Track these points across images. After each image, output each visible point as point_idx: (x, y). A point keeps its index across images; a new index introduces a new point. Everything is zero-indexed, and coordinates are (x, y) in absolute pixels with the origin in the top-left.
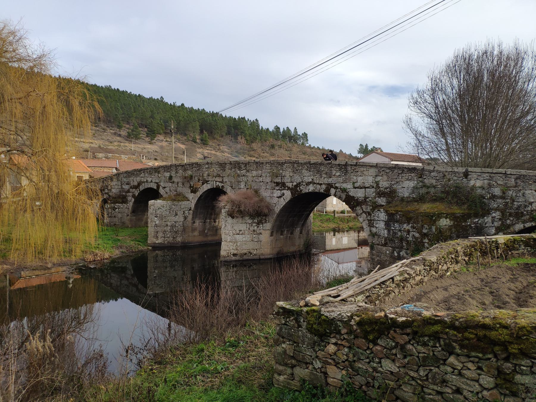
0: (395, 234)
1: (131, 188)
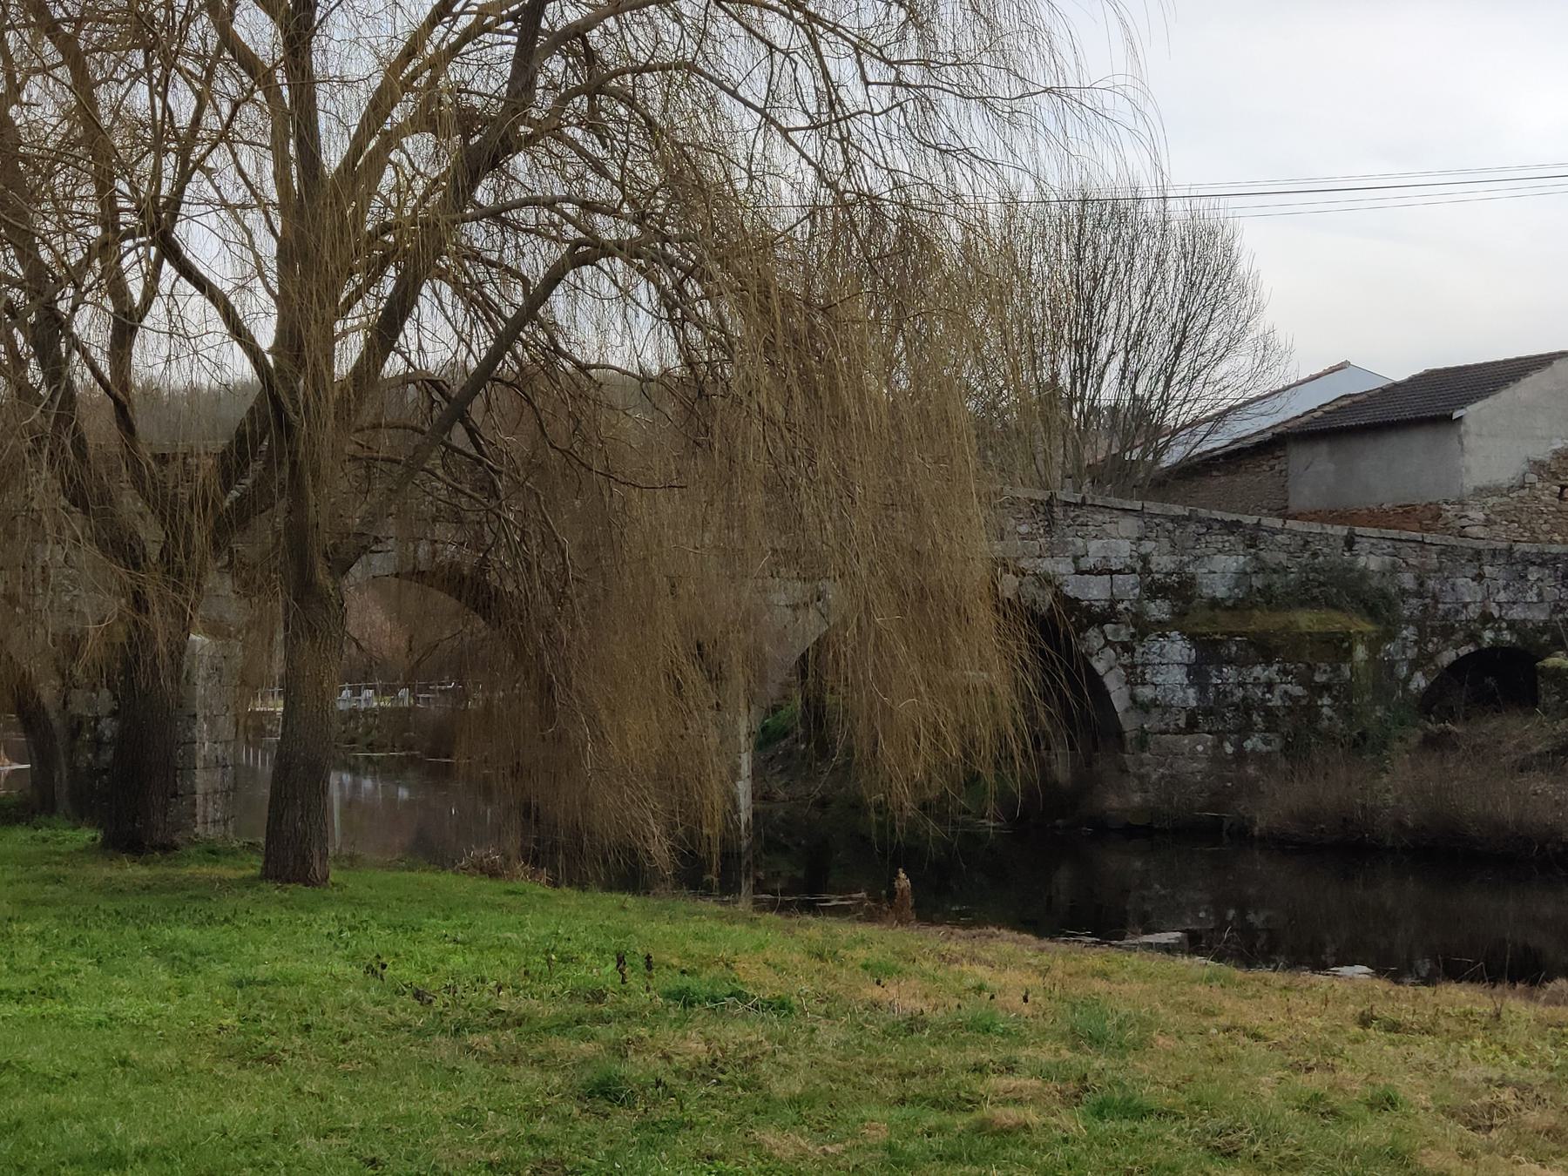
0: (1226, 697)
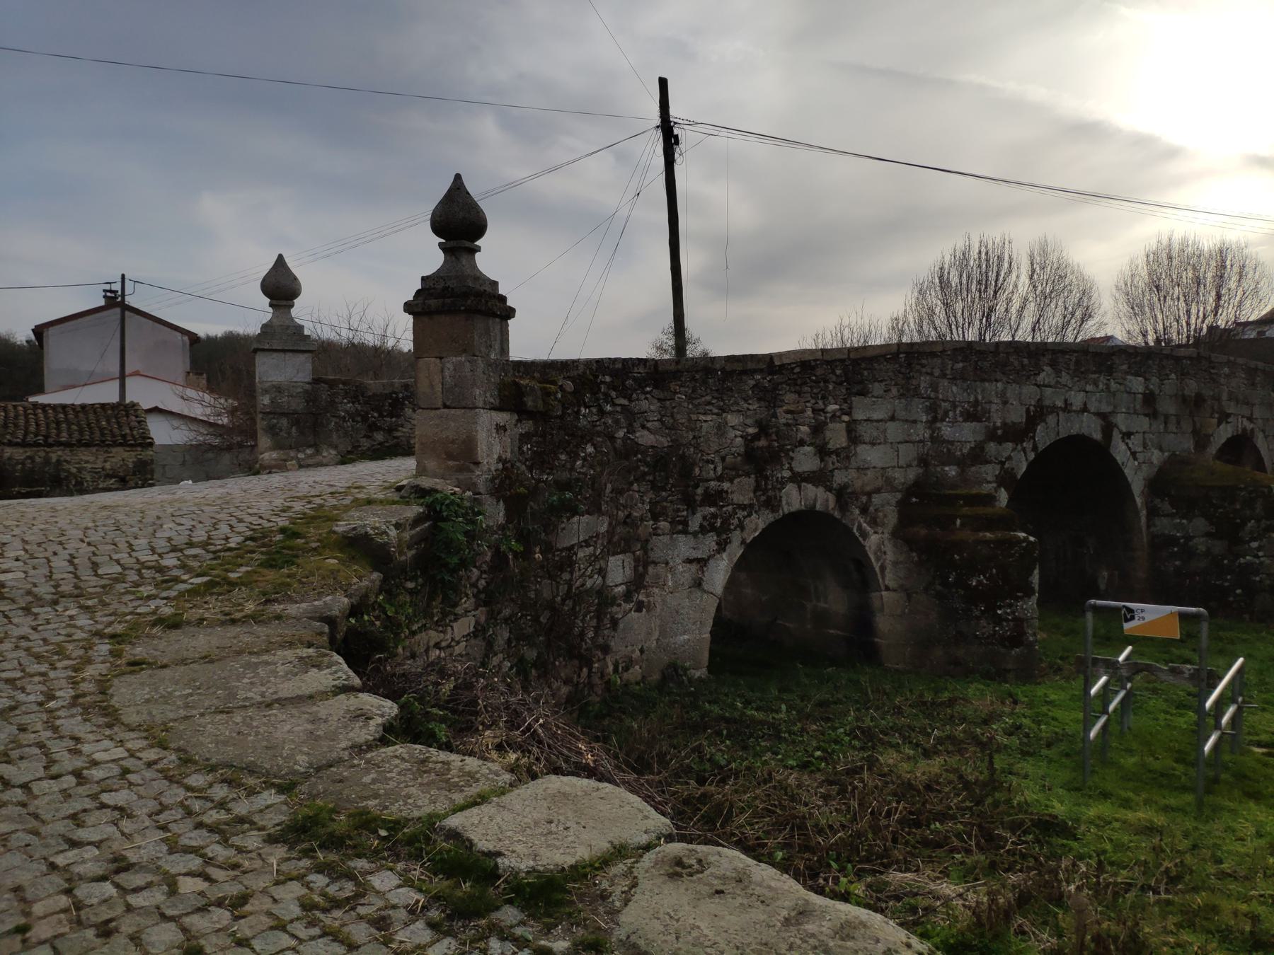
1: (992, 436)
